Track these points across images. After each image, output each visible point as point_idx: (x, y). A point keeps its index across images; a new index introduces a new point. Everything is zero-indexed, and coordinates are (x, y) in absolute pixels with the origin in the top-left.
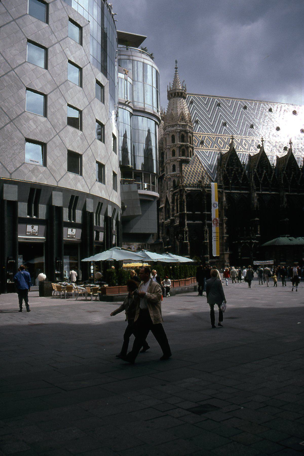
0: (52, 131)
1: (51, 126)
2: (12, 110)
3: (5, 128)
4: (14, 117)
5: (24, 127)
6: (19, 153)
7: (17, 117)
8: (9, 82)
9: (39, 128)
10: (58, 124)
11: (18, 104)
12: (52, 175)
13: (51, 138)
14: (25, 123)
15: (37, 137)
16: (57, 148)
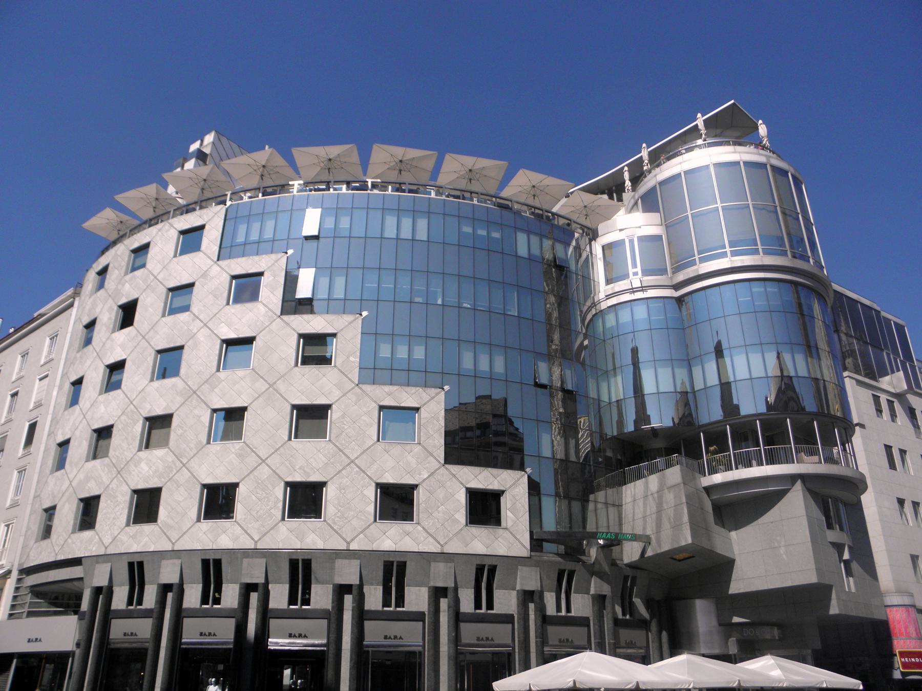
0: (175, 464)
1: (174, 457)
2: (122, 459)
3: (111, 486)
4: (122, 466)
5: (133, 475)
6: (121, 514)
7: (126, 464)
8: (125, 420)
9: (154, 468)
10: (188, 449)
11: (131, 447)
12: (165, 534)
13: (171, 475)
14: (134, 468)
15: (148, 483)
16: (182, 489)
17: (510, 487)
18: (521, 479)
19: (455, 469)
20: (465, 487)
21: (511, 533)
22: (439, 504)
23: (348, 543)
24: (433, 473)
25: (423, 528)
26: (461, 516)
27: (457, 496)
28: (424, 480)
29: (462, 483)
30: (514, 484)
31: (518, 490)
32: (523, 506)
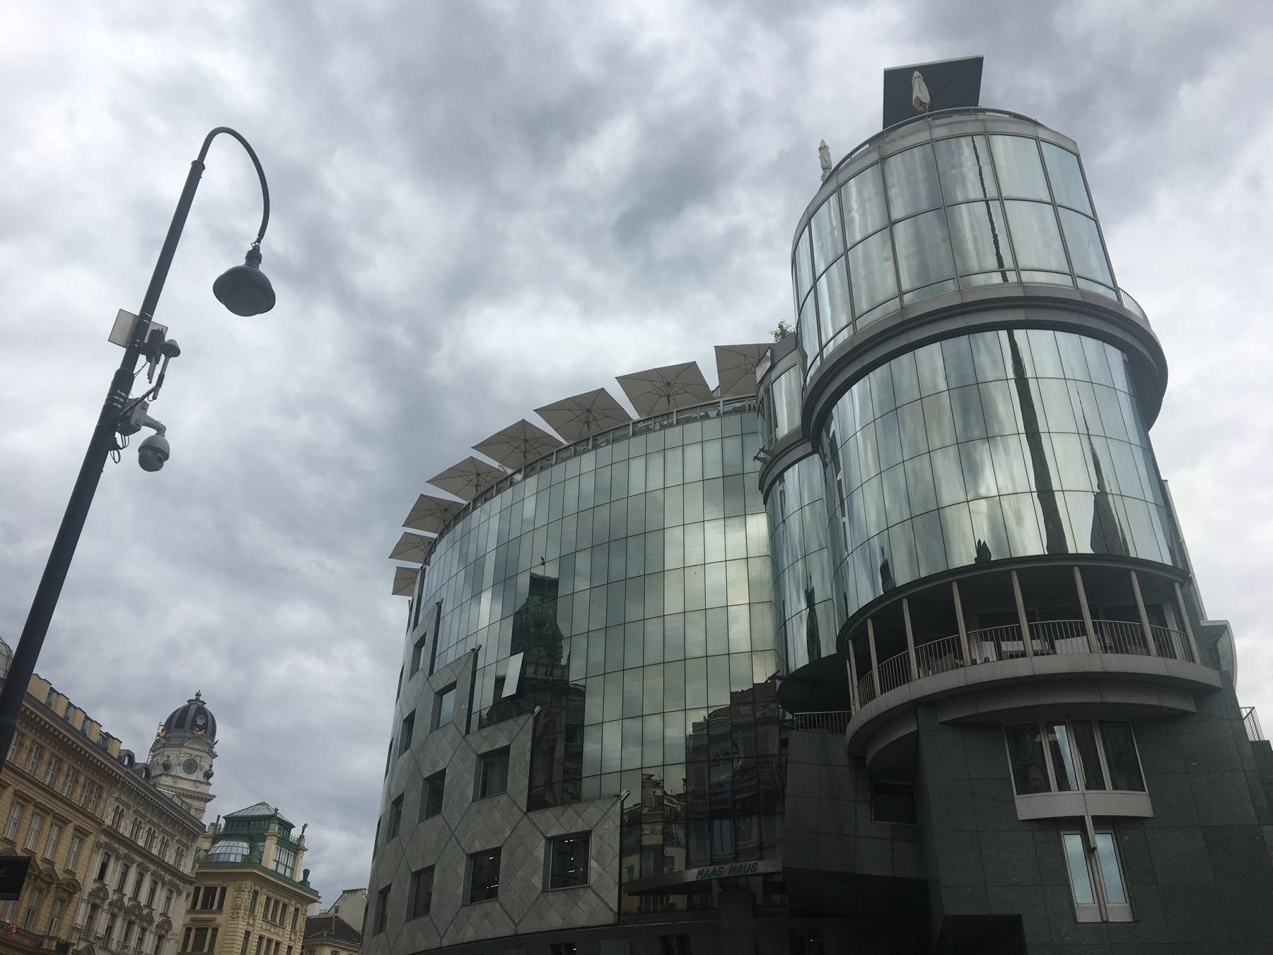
17: (596, 825)
18: (613, 809)
19: (535, 815)
20: (549, 839)
21: (594, 891)
22: (518, 868)
23: (441, 939)
24: (515, 827)
25: (500, 904)
26: (537, 881)
27: (535, 853)
28: (508, 837)
29: (542, 833)
30: (603, 817)
31: (606, 826)
32: (613, 849)
